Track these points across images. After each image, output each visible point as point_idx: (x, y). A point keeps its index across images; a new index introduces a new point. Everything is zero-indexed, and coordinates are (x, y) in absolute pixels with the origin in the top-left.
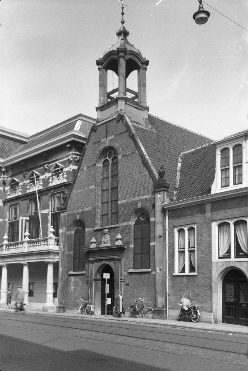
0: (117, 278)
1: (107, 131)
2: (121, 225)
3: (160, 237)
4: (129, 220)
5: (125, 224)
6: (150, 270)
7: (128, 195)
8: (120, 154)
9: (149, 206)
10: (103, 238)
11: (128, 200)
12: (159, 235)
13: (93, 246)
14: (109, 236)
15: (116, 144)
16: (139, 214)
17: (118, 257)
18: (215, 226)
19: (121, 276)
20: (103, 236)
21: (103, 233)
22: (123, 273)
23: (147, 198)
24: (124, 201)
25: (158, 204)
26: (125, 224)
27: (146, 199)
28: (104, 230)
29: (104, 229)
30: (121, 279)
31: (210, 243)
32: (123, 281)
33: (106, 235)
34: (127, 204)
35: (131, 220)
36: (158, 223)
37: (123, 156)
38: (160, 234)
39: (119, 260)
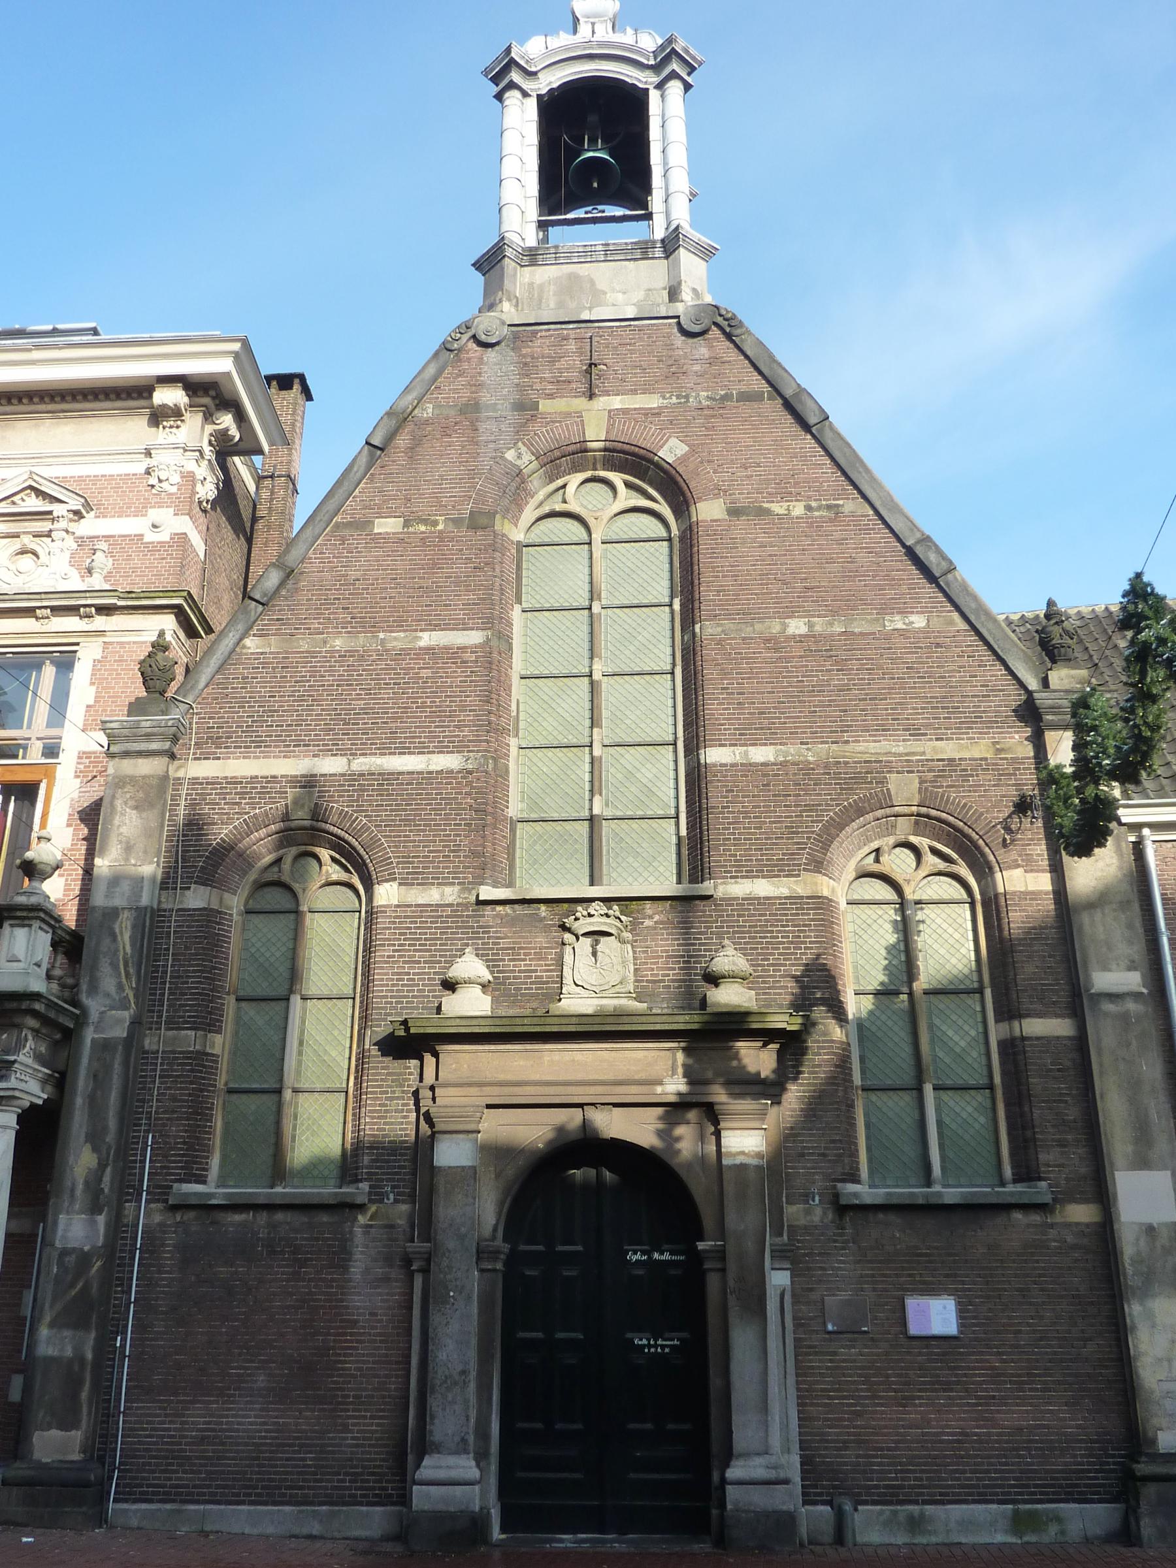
4: (818, 866)
13: (471, 1004)
21: (564, 928)
24: (761, 754)
26: (762, 888)
37: (734, 512)
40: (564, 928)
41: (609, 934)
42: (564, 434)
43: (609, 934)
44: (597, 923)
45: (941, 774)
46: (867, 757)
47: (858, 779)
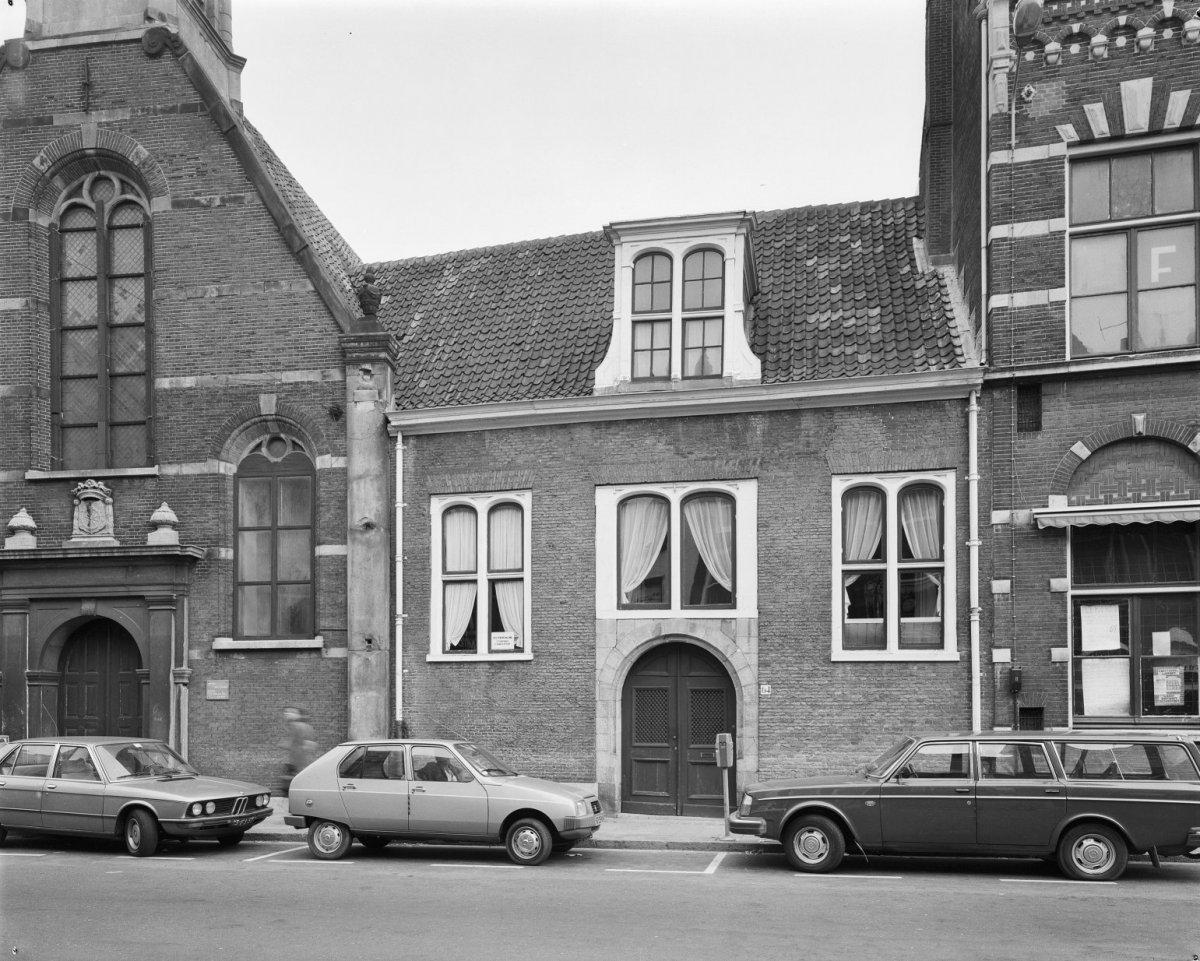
0: (161, 671)
1: (87, 86)
2: (171, 470)
3: (369, 526)
4: (216, 455)
5: (190, 469)
6: (318, 642)
7: (209, 361)
8: (161, 193)
9: (313, 411)
10: (80, 513)
11: (207, 378)
12: (366, 521)
14: (110, 508)
15: (140, 147)
16: (262, 438)
17: (169, 593)
18: (606, 500)
19: (179, 663)
20: (74, 506)
21: (75, 496)
22: (185, 654)
23: (303, 383)
24: (188, 382)
25: (360, 407)
27: (297, 383)
28: (81, 485)
29: (83, 480)
30: (178, 675)
31: (589, 558)
32: (186, 681)
33: (95, 506)
34: (205, 392)
35: (223, 454)
36: (360, 477)
37: (177, 204)
38: (371, 517)
39: (169, 601)
40: (75, 496)
41: (97, 500)
42: (69, 143)
43: (97, 500)
44: (90, 493)
45: (290, 393)
46: (247, 383)
47: (242, 397)
